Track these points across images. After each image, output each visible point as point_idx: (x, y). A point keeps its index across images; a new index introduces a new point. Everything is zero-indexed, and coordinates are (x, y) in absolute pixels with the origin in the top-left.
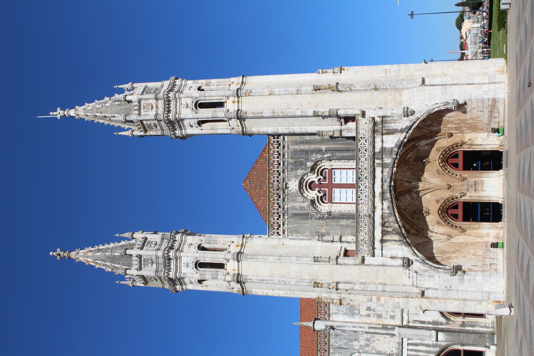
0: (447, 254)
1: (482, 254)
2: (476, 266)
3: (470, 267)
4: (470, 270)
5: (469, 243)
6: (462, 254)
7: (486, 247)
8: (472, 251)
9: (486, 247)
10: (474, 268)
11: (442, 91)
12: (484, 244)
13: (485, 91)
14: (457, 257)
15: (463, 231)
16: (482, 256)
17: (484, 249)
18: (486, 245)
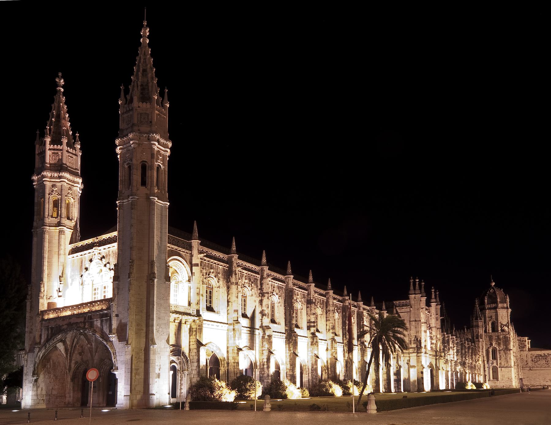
0: (53, 371)
1: (53, 393)
2: (42, 390)
3: (41, 386)
4: (38, 387)
5: (64, 385)
6: (53, 380)
7: (60, 396)
8: (56, 387)
9: (60, 396)
10: (40, 389)
11: (123, 361)
12: (63, 394)
13: (121, 393)
14: (50, 377)
15: (73, 379)
16: (52, 394)
17: (58, 395)
18: (62, 396)
